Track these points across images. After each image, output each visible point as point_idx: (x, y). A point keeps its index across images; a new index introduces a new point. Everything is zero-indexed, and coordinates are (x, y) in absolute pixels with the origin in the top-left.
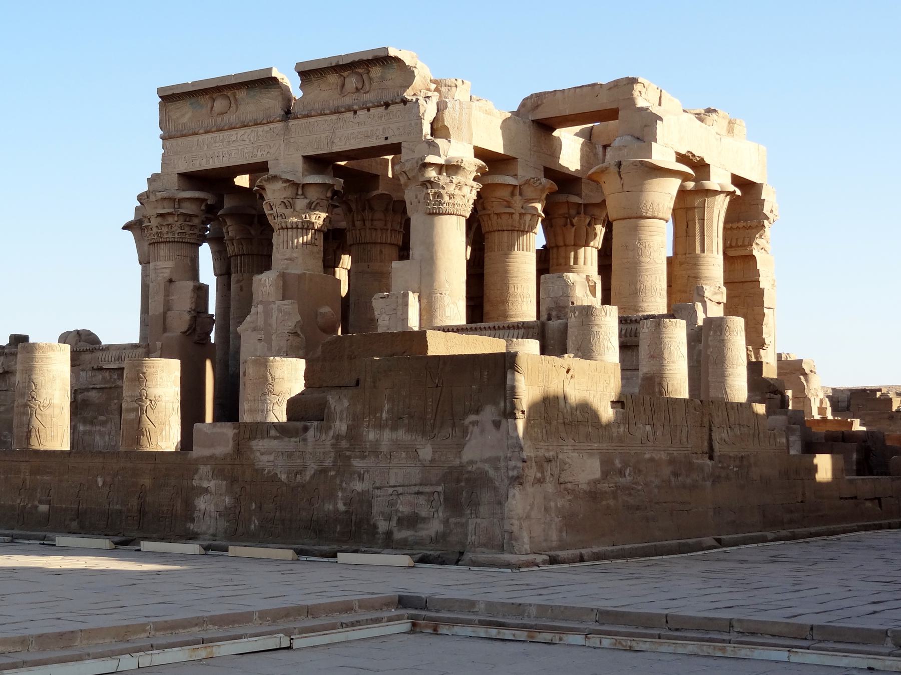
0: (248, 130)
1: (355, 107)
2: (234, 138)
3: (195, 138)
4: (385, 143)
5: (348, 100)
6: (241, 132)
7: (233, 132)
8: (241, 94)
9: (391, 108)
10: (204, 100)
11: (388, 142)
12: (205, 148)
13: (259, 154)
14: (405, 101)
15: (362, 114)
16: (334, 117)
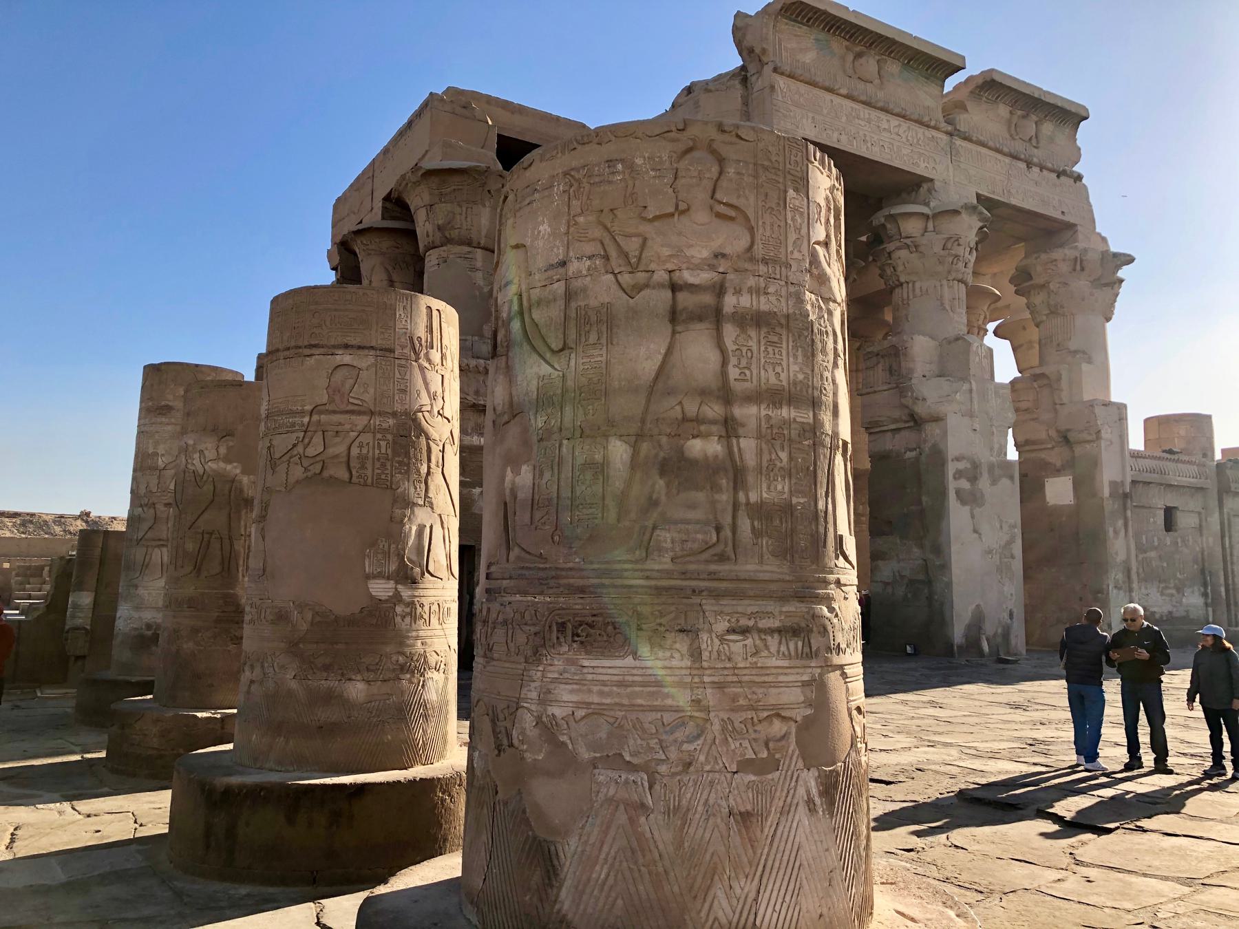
0: (905, 125)
1: (1035, 160)
2: (885, 125)
3: (828, 96)
4: (1060, 217)
5: (1019, 147)
6: (895, 121)
7: (883, 116)
8: (893, 67)
9: (1062, 178)
10: (838, 45)
11: (1066, 218)
12: (844, 119)
13: (923, 165)
14: (1079, 178)
15: (1036, 170)
16: (1007, 160)
